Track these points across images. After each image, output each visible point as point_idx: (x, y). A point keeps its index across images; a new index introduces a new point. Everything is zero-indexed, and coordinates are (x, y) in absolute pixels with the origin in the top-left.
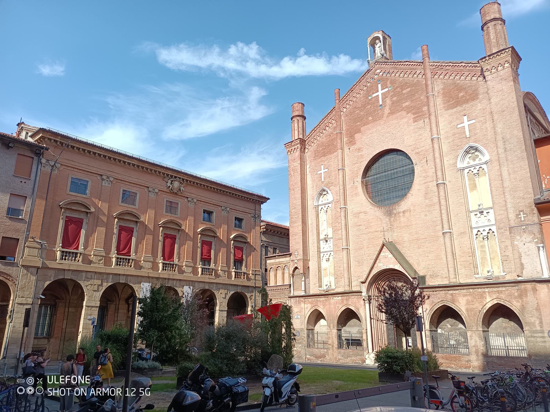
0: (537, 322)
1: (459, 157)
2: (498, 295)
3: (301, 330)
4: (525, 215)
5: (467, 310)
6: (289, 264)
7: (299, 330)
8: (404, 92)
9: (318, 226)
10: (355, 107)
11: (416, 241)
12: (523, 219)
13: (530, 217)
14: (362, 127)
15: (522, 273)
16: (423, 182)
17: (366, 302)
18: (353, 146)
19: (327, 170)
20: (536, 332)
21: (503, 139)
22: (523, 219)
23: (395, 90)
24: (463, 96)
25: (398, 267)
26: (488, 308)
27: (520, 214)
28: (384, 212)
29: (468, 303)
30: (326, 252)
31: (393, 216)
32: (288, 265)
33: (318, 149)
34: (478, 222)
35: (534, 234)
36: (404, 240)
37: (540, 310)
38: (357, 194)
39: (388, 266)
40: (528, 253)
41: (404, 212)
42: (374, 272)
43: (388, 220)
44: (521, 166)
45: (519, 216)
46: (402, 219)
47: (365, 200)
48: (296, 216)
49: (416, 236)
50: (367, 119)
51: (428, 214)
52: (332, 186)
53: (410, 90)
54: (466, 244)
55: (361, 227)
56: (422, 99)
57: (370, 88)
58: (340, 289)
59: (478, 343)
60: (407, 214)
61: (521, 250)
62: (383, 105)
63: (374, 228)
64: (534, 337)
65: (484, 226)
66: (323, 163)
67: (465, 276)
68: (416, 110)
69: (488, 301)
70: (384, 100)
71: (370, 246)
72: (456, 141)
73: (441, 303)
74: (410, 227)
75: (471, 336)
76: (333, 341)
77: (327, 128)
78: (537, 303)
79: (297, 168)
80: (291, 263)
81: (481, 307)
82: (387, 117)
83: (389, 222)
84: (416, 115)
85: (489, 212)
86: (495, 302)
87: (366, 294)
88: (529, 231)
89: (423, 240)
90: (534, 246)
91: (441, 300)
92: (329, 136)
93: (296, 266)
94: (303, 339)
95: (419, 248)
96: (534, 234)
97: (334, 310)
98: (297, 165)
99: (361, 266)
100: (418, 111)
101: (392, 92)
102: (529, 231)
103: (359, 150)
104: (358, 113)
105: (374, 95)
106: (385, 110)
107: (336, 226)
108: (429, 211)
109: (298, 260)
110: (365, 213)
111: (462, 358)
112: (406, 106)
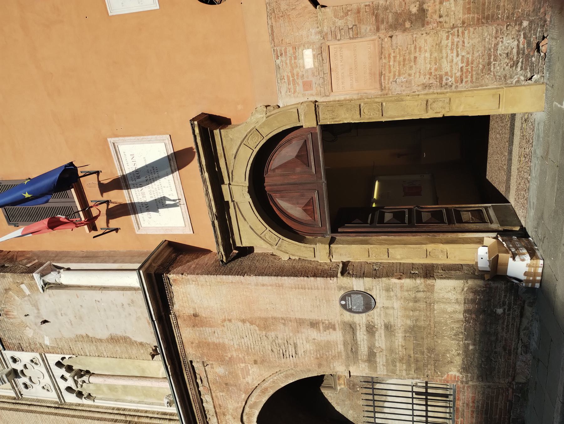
37: (266, 319)
78: (244, 321)
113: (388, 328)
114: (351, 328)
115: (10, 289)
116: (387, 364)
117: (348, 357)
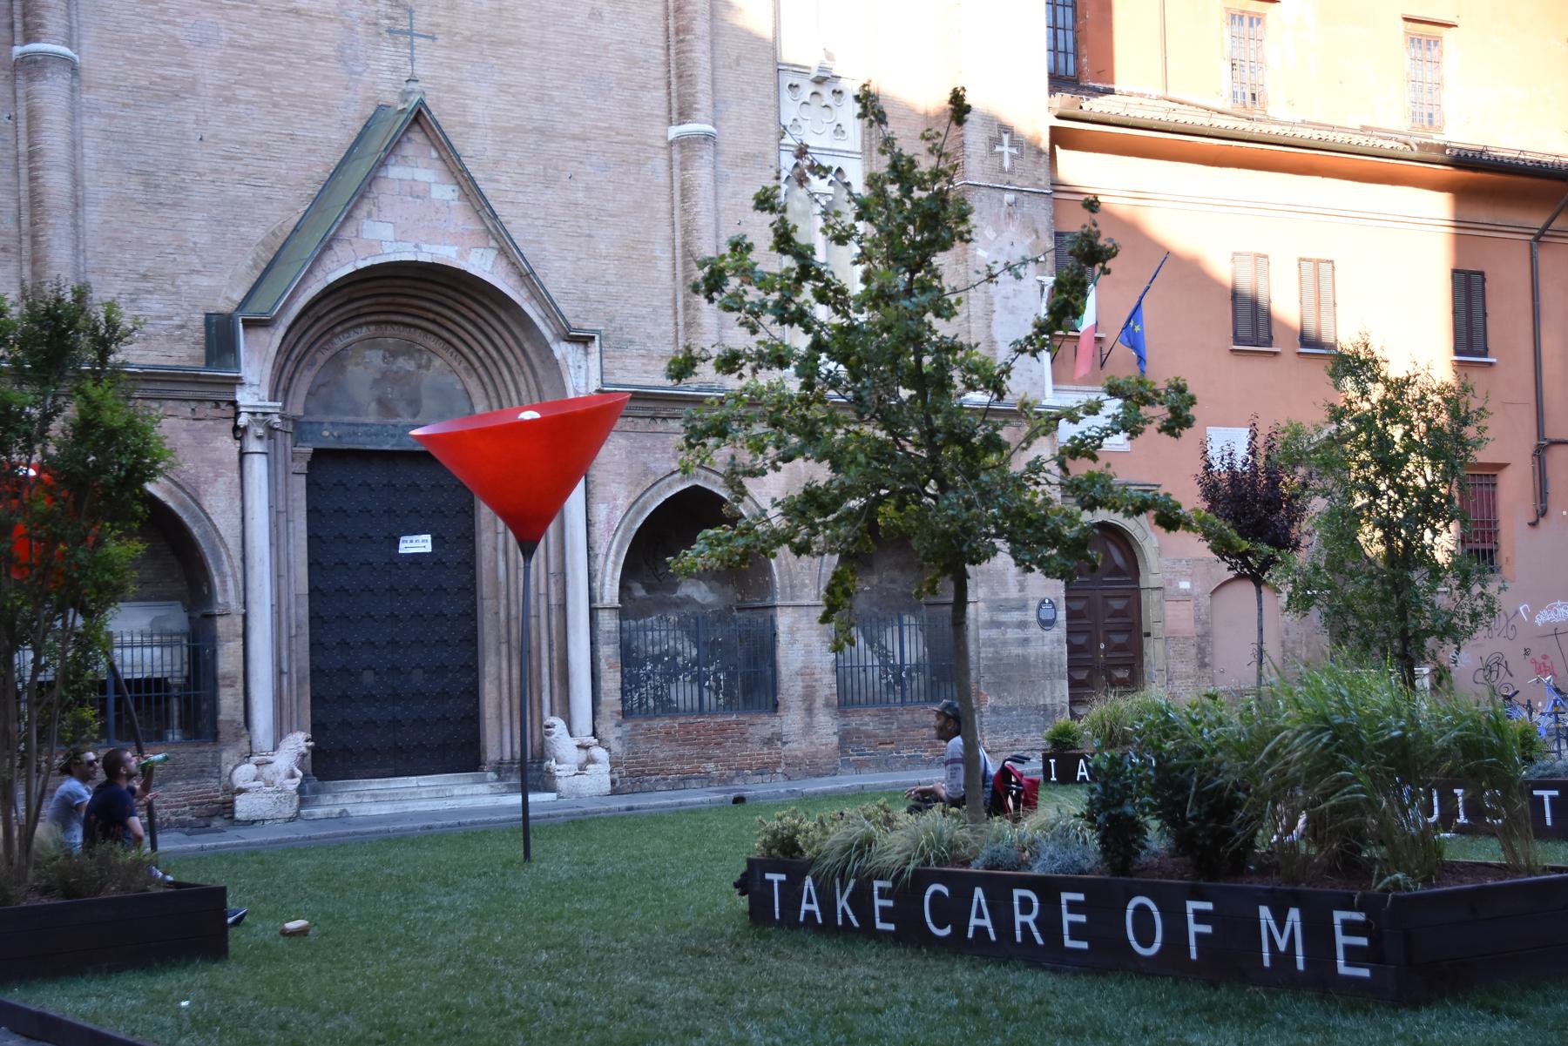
4: (1014, 151)
11: (532, 138)
12: (1007, 164)
17: (253, 445)
22: (1007, 164)
25: (482, 264)
27: (999, 142)
34: (800, 122)
35: (1036, 232)
36: (470, 119)
39: (425, 247)
40: (1012, 302)
42: (338, 267)
45: (998, 149)
59: (817, 657)
71: (245, 93)
74: (510, 51)
75: (792, 632)
85: (797, 86)
87: (265, 393)
89: (572, 143)
95: (548, 182)
96: (1036, 232)
99: (165, 212)
102: (1023, 215)
111: (751, 730)
113: (1025, 642)
114: (1023, 607)
115: (1038, 237)
116: (990, 639)
117: (993, 601)
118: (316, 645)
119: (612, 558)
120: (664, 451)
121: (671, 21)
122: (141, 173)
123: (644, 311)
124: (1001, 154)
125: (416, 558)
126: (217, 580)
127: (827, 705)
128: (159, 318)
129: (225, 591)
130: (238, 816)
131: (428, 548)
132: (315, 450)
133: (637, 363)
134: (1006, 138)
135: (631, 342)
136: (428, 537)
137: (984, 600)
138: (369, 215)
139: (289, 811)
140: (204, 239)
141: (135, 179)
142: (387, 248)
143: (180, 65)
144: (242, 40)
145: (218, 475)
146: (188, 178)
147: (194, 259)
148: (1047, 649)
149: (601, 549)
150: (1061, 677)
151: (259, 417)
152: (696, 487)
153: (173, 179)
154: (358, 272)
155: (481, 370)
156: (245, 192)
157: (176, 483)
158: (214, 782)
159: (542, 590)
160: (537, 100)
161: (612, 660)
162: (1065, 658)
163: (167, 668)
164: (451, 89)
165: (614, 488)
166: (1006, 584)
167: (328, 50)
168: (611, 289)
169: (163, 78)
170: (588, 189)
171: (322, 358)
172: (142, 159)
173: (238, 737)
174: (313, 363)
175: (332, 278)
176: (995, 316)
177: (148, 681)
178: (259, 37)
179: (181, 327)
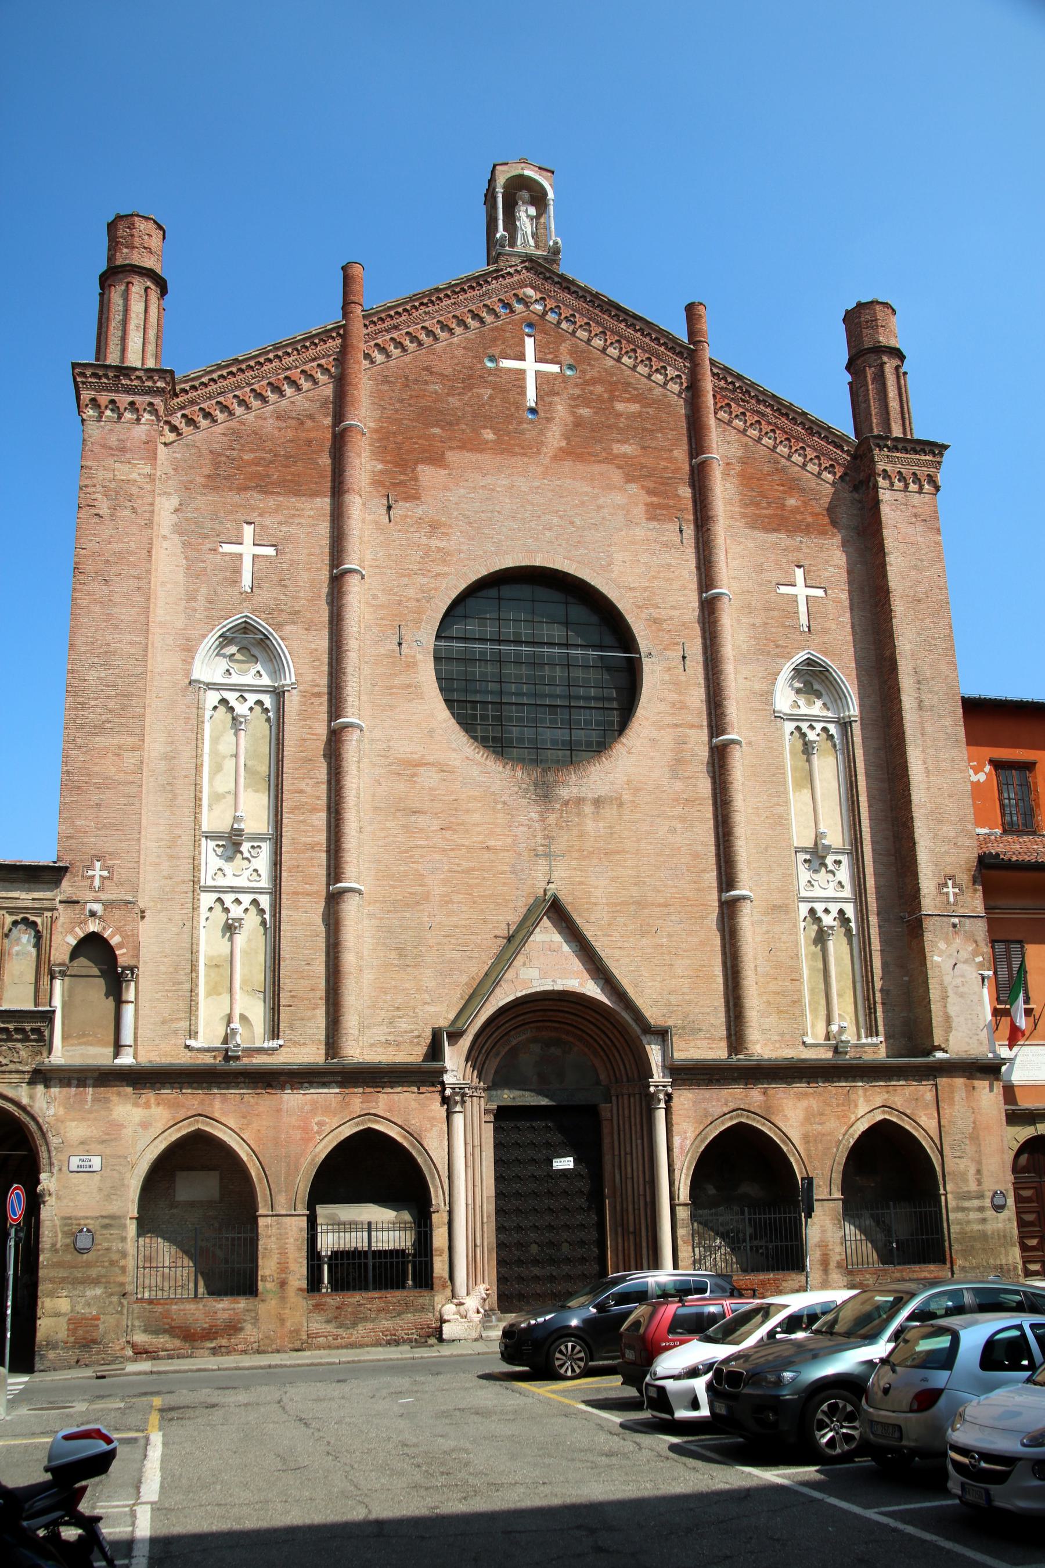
0: (972, 1171)
1: (779, 678)
2: (886, 1096)
3: (107, 1221)
4: (957, 890)
5: (806, 1139)
6: (49, 914)
7: (92, 1224)
8: (620, 407)
9: (198, 768)
10: (427, 369)
11: (633, 908)
12: (952, 899)
13: (968, 896)
14: (451, 448)
15: (947, 1040)
16: (670, 720)
18: (407, 505)
19: (270, 551)
20: (967, 1196)
21: (916, 672)
22: (952, 899)
23: (587, 383)
24: (795, 510)
25: (592, 989)
26: (859, 1133)
27: (946, 885)
28: (524, 786)
29: (809, 1117)
30: (233, 890)
31: (558, 806)
32: (38, 920)
33: (235, 453)
36: (593, 900)
38: (412, 690)
39: (559, 981)
40: (961, 989)
41: (598, 802)
42: (503, 996)
43: (534, 816)
44: (953, 760)
45: (945, 890)
46: (590, 825)
47: (445, 721)
48: (111, 704)
49: (635, 891)
50: (475, 431)
51: (679, 826)
52: (294, 623)
53: (640, 413)
54: (784, 943)
55: (422, 821)
56: (676, 459)
57: (492, 330)
58: (304, 1050)
59: (829, 1234)
60: (609, 812)
61: (947, 979)
62: (542, 414)
63: (479, 834)
64: (963, 1209)
65: (827, 900)
66: (254, 516)
67: (777, 1038)
68: (655, 482)
69: (861, 1113)
70: (547, 399)
71: (456, 898)
72: (773, 630)
73: (731, 1118)
74: (618, 857)
76: (283, 1268)
77: (289, 391)
79: (134, 490)
80: (64, 915)
81: (843, 1130)
82: (555, 458)
83: (538, 826)
84: (655, 499)
86: (879, 1116)
88: (965, 932)
90: (975, 975)
91: (732, 1106)
92: (293, 423)
93: (93, 927)
94: (112, 1263)
96: (976, 942)
97: (298, 1135)
98: (134, 476)
100: (662, 488)
101: (577, 385)
102: (965, 932)
103: (434, 526)
104: (436, 393)
105: (506, 364)
106: (549, 434)
107: (301, 792)
108: (683, 819)
109: (109, 905)
110: (443, 768)
112: (625, 455)
113: (984, 1220)
114: (981, 1196)
117: (958, 1193)
118: (500, 1229)
119: (684, 1171)
120: (718, 1100)
121: (720, 830)
122: (397, 949)
123: (708, 1010)
124: (947, 893)
125: (564, 1172)
126: (432, 1190)
127: (839, 1266)
128: (406, 1032)
129: (437, 1196)
130: (444, 1336)
131: (571, 1165)
132: (498, 1107)
133: (705, 1043)
134: (950, 883)
135: (700, 1030)
136: (571, 1159)
137: (952, 1193)
138: (524, 964)
139: (475, 1335)
140: (432, 984)
141: (393, 952)
142: (535, 983)
143: (420, 885)
144: (456, 868)
145: (433, 1126)
146: (423, 949)
147: (427, 996)
148: (1000, 1225)
149: (677, 1166)
150: (1013, 1245)
151: (457, 1090)
152: (741, 1123)
153: (415, 951)
154: (517, 999)
155: (602, 1053)
156: (456, 955)
157: (408, 1132)
158: (430, 1315)
159: (641, 1192)
160: (635, 884)
161: (685, 1238)
162: (1016, 1232)
163: (403, 1244)
164: (581, 883)
165: (685, 1125)
166: (968, 1180)
167: (507, 868)
168: (687, 997)
169: (411, 894)
170: (670, 936)
171: (504, 1051)
172: (398, 940)
173: (444, 1287)
174: (498, 1054)
175: (501, 1003)
176: (949, 1000)
177: (391, 1251)
178: (465, 865)
179: (419, 1036)
